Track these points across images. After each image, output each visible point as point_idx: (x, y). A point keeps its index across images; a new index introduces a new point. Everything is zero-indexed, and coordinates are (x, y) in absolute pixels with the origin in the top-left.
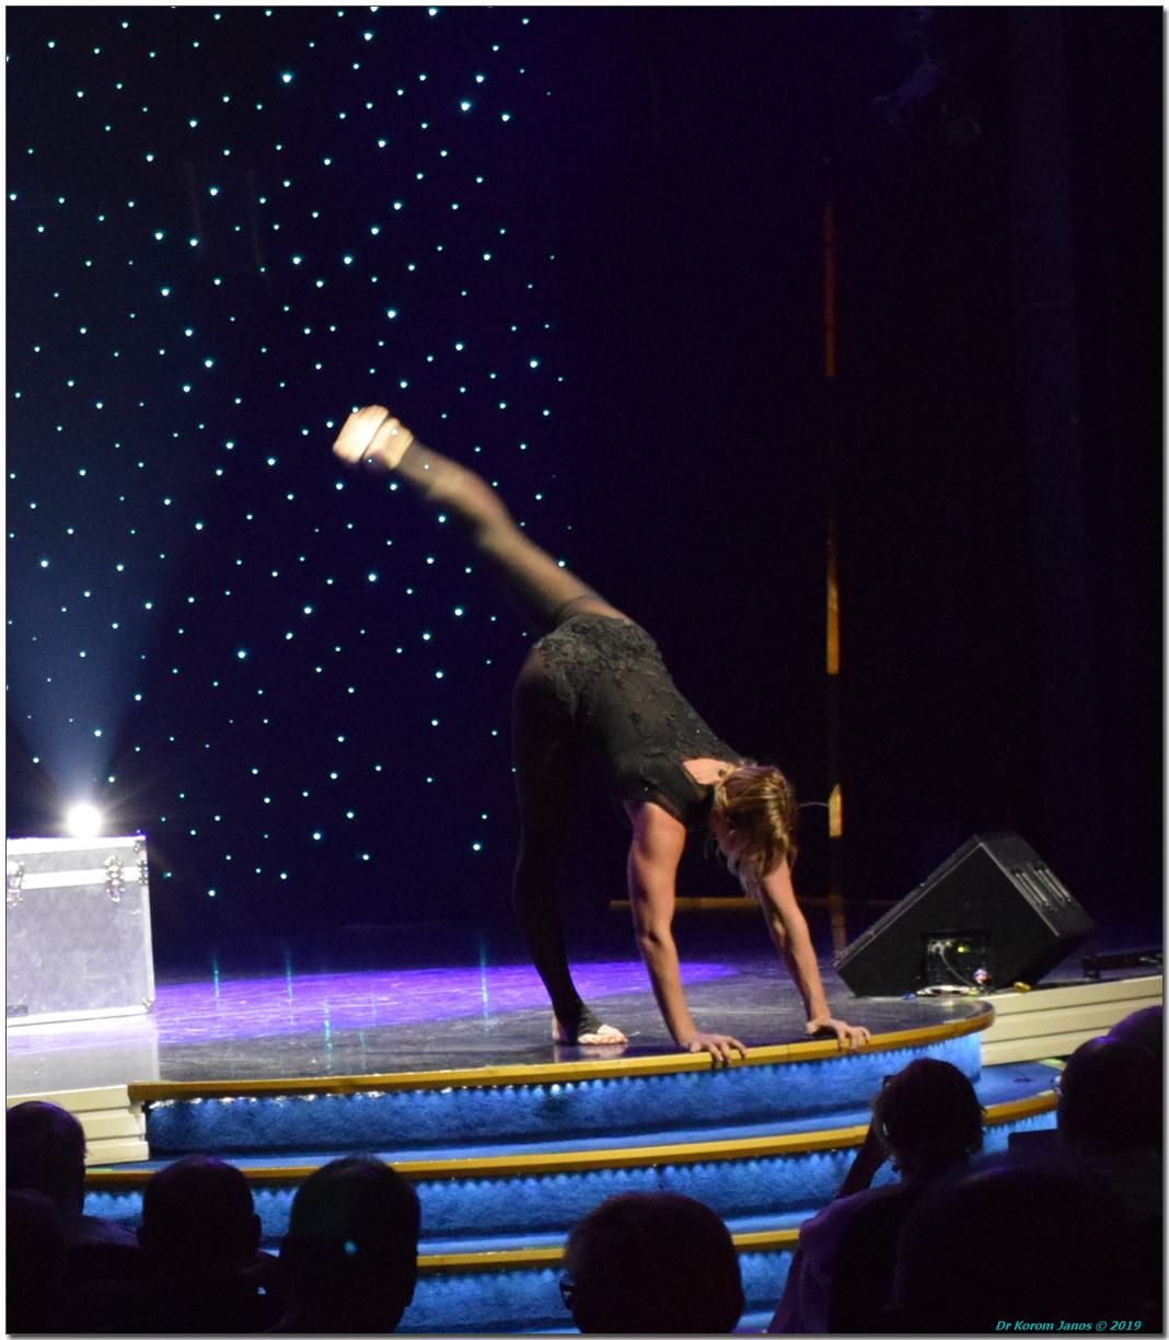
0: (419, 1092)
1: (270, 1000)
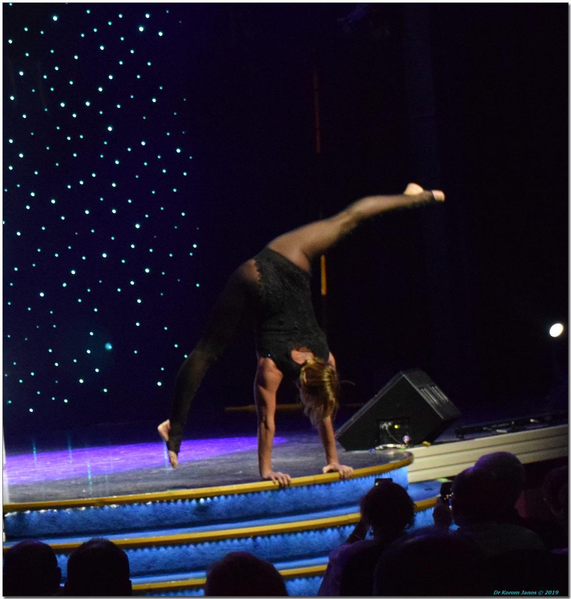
0: (136, 504)
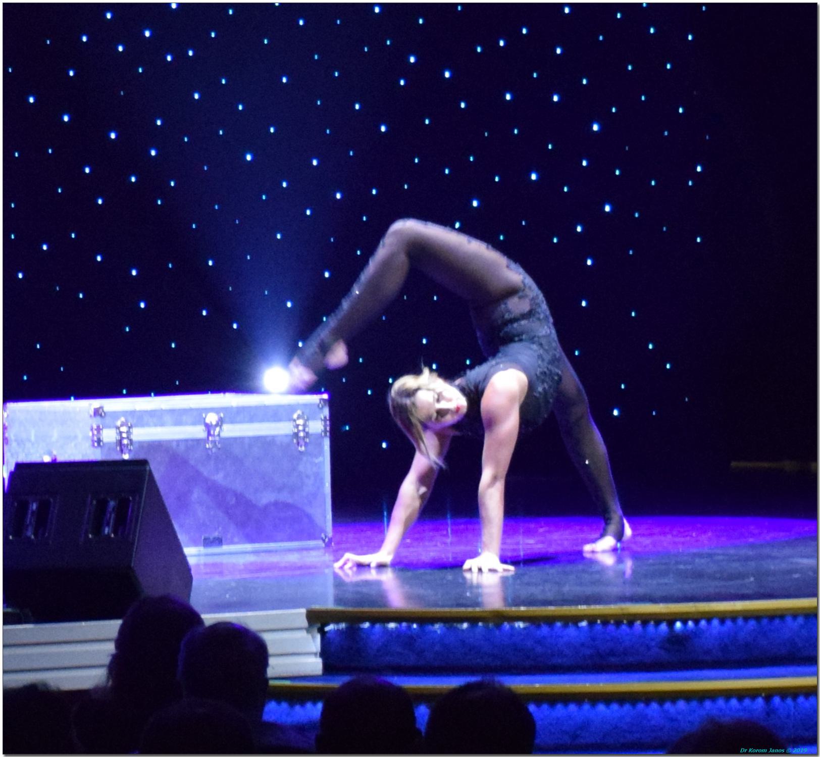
0: (559, 624)
1: (431, 539)
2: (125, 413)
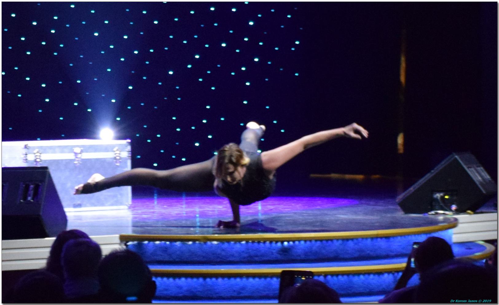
0: (232, 242)
1: (176, 206)
2: (38, 147)
